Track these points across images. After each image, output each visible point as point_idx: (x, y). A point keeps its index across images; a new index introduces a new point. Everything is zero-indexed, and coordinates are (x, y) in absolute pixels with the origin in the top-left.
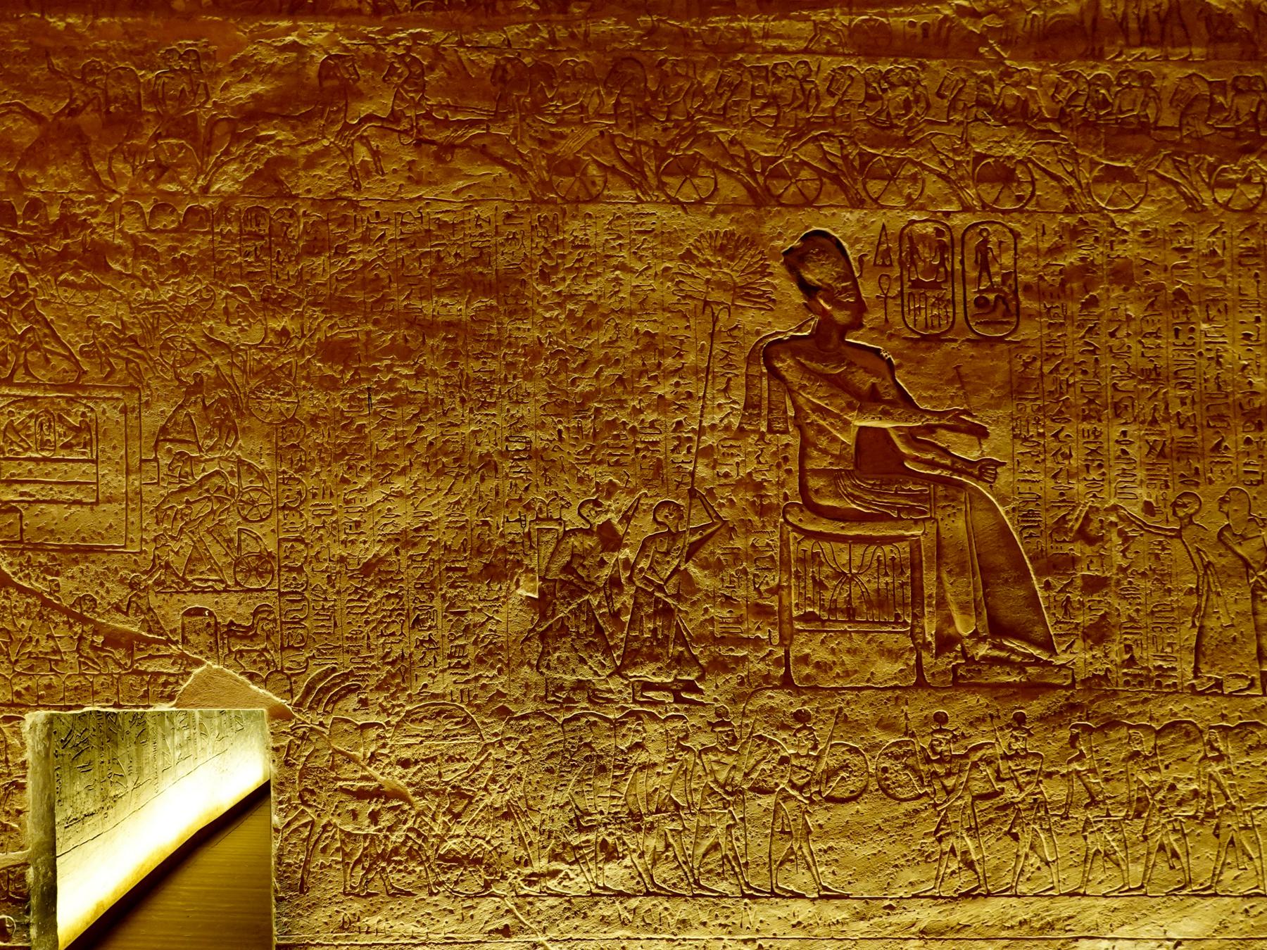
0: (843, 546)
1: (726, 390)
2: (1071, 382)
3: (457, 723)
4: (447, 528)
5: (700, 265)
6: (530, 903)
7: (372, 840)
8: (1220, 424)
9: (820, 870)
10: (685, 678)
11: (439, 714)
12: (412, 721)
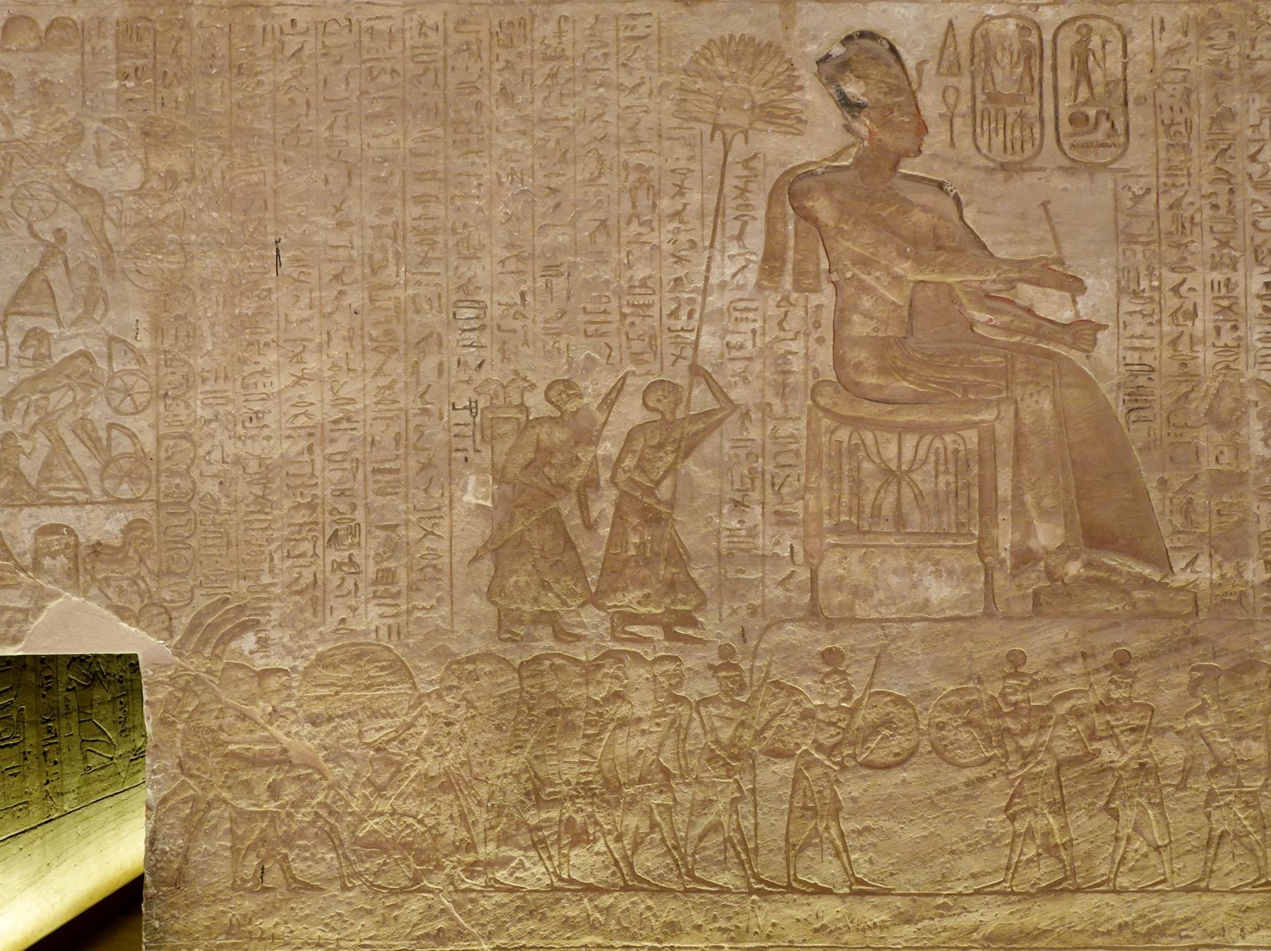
0: (889, 436)
1: (740, 237)
2: (1197, 218)
3: (382, 668)
4: (375, 419)
5: (708, 78)
6: (472, 901)
7: (273, 820)
9: (853, 857)
10: (680, 607)
11: (359, 656)
12: (325, 667)
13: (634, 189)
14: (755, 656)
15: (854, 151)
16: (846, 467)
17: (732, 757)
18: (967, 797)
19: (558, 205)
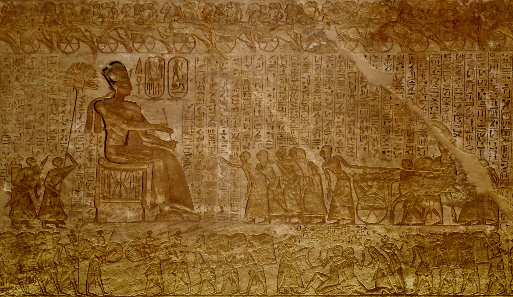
1: (80, 118)
2: (205, 112)
8: (259, 127)
13: (52, 105)
14: (80, 232)
15: (112, 94)
16: (106, 181)
17: (73, 260)
18: (135, 270)
19: (31, 109)
